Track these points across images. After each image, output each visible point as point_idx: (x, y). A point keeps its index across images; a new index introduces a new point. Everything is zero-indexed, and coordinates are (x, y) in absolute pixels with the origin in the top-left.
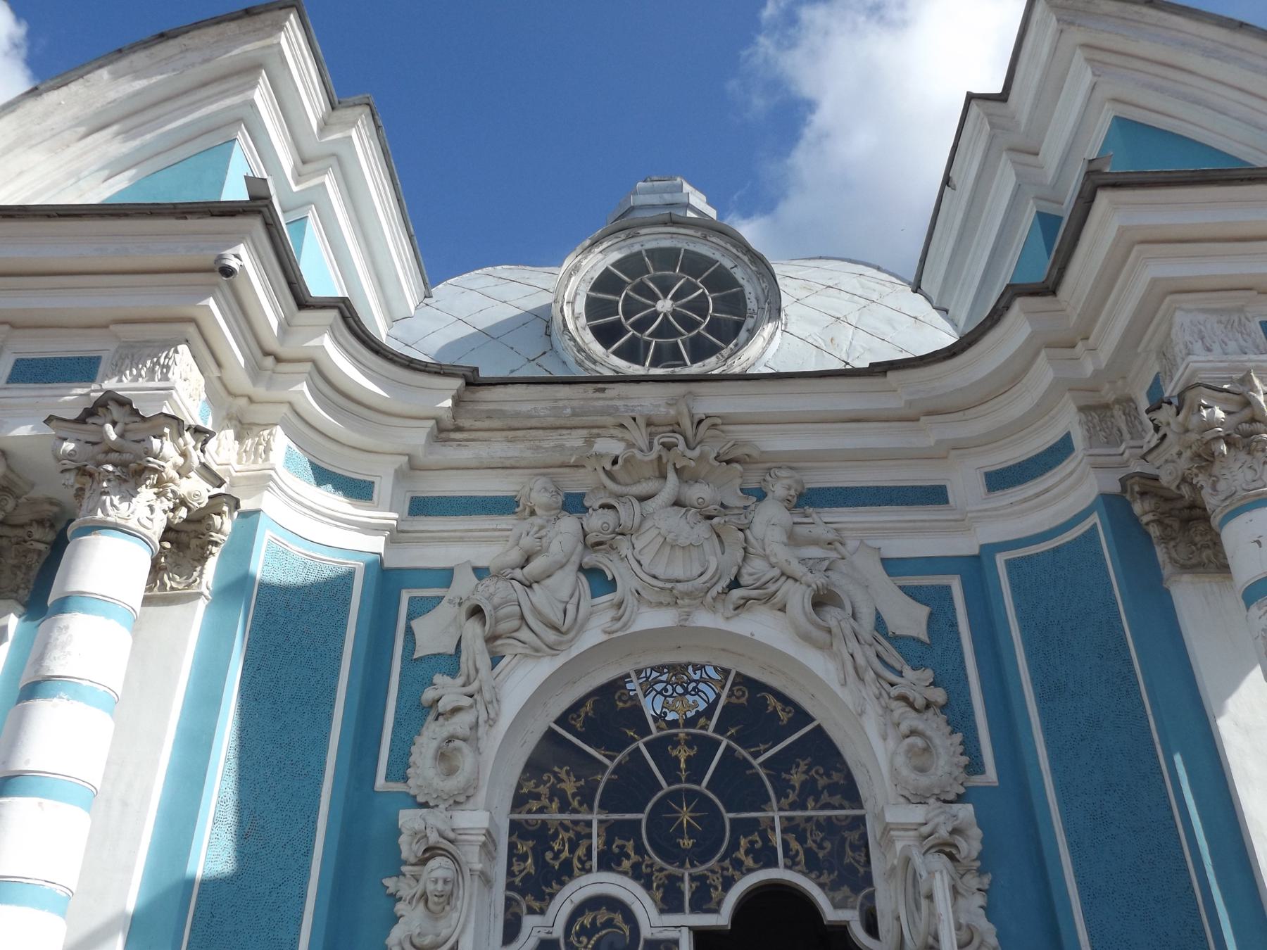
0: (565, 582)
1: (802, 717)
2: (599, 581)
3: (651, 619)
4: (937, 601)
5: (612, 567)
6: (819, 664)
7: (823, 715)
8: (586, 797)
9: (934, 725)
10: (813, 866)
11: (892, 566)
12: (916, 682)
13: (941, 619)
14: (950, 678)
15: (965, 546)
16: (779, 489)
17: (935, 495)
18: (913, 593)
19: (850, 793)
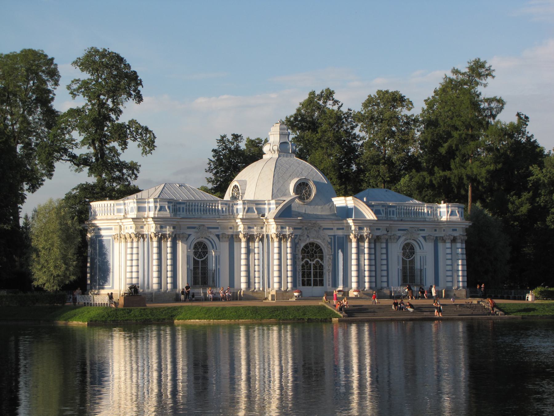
0: (306, 237)
1: (320, 247)
2: (308, 237)
3: (312, 240)
4: (331, 239)
5: (309, 236)
6: (323, 244)
7: (322, 247)
8: (305, 253)
9: (330, 249)
10: (319, 258)
11: (329, 236)
12: (329, 246)
13: (331, 241)
14: (331, 246)
15: (333, 234)
16: (322, 229)
17: (332, 229)
18: (330, 238)
19: (322, 253)
